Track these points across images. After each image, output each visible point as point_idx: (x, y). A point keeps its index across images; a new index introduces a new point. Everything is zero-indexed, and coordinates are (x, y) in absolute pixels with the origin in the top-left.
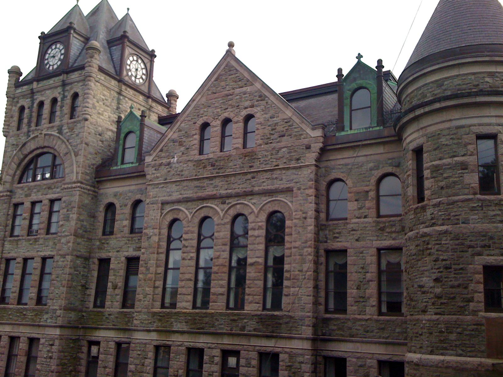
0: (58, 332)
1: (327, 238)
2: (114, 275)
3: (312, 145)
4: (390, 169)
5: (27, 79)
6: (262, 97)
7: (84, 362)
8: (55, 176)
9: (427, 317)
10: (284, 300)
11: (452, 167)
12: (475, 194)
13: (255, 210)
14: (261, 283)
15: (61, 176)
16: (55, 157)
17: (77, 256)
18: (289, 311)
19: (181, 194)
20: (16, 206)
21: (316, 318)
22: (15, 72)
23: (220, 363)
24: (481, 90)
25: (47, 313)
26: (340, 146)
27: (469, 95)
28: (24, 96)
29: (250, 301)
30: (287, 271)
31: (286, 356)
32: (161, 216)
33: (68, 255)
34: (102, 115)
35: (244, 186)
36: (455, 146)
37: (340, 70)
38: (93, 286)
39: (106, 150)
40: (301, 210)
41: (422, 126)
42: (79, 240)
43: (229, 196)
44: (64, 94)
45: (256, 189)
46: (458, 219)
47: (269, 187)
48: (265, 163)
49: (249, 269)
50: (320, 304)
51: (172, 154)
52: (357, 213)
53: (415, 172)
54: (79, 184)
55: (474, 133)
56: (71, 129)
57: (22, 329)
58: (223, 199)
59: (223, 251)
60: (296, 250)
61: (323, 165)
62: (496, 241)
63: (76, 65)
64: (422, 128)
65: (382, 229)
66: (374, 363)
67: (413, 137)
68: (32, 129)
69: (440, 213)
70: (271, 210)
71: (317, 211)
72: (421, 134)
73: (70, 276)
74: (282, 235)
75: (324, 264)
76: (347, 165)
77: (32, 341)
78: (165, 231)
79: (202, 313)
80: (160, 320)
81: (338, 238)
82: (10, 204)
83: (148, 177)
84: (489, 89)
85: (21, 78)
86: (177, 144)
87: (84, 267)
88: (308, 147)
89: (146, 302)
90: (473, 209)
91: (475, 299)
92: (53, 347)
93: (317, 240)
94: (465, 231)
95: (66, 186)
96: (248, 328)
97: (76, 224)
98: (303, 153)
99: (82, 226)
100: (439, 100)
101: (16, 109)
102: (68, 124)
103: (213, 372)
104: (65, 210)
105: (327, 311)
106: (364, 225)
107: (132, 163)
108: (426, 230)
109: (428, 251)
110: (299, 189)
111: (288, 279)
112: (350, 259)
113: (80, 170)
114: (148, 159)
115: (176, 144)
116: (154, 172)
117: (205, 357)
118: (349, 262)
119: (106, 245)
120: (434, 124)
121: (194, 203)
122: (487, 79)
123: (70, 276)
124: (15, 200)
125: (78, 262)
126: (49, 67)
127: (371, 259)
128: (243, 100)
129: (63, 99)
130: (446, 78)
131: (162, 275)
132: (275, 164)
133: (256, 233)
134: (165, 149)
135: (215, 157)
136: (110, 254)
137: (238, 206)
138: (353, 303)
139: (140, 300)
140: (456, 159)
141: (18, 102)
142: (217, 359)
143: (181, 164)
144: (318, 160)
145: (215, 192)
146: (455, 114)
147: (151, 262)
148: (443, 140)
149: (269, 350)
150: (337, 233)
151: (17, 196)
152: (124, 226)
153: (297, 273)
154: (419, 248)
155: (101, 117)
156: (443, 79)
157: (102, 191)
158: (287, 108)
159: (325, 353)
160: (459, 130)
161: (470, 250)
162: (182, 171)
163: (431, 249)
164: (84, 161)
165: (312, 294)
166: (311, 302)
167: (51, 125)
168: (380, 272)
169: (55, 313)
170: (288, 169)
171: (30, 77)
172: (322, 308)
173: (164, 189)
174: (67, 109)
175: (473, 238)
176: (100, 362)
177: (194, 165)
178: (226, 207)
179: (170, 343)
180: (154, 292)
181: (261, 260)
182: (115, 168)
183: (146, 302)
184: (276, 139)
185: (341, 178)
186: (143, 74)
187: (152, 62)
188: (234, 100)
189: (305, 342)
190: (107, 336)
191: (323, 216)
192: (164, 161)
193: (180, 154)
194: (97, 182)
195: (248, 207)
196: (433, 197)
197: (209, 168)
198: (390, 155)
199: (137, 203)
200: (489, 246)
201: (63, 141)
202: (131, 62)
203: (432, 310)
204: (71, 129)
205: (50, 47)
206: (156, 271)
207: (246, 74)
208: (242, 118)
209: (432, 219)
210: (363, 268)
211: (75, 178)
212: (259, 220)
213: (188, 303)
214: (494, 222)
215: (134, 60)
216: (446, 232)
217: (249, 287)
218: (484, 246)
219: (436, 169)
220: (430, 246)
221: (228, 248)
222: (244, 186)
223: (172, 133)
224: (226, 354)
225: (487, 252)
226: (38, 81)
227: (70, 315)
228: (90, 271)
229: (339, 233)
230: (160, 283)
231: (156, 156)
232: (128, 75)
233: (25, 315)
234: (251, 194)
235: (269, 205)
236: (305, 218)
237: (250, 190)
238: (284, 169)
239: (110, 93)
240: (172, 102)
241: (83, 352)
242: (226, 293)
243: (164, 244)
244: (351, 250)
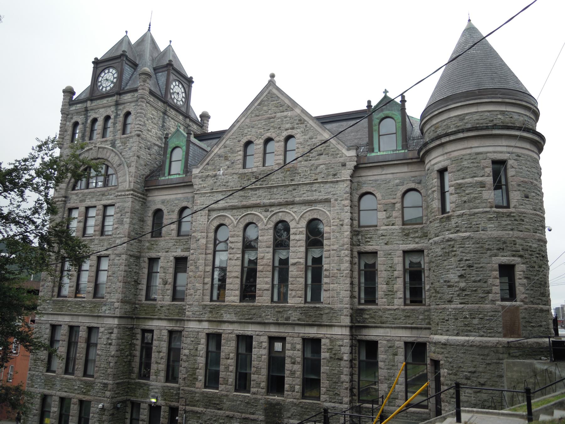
0: (116, 321)
1: (359, 242)
2: (164, 273)
3: (347, 163)
4: (413, 186)
5: (80, 98)
6: (301, 121)
7: (138, 348)
8: (107, 185)
9: (453, 306)
10: (324, 295)
11: (472, 185)
12: (491, 207)
13: (296, 217)
14: (302, 280)
15: (113, 184)
16: (107, 167)
17: (131, 256)
18: (329, 304)
19: (227, 203)
20: (70, 210)
21: (352, 309)
22: (69, 92)
23: (267, 348)
24: (495, 125)
25: (105, 305)
26: (371, 165)
27: (487, 128)
28: (78, 113)
29: (293, 295)
30: (326, 270)
31: (328, 341)
32: (208, 221)
33: (123, 254)
34: (151, 131)
35: (286, 196)
36: (474, 168)
37: (369, 102)
38: (144, 281)
39: (153, 162)
40: (338, 218)
41: (446, 151)
43: (272, 205)
44: (117, 113)
45: (297, 199)
46: (478, 227)
47: (309, 198)
48: (305, 177)
49: (291, 268)
50: (355, 297)
51: (218, 167)
52: (385, 221)
53: (439, 188)
55: (490, 158)
56: (124, 143)
57: (81, 319)
58: (266, 207)
59: (268, 253)
60: (334, 252)
61: (355, 180)
62: (509, 245)
63: (128, 87)
64: (446, 153)
65: (407, 235)
66: (402, 344)
67: (437, 160)
69: (463, 222)
70: (311, 218)
71: (352, 219)
72: (446, 158)
74: (320, 239)
75: (357, 264)
76: (376, 181)
77: (90, 330)
78: (212, 235)
79: (249, 306)
80: (211, 312)
81: (369, 242)
82: (65, 208)
83: (195, 187)
84: (501, 124)
85: (75, 97)
87: (136, 265)
88: (344, 165)
89: (197, 297)
90: (490, 219)
91: (494, 291)
92: (112, 335)
93: (352, 244)
94: (484, 237)
95: (119, 194)
96: (292, 318)
97: (130, 227)
98: (339, 170)
100: (463, 131)
101: (70, 124)
102: (121, 139)
103: (262, 355)
104: (119, 215)
105: (360, 303)
106: (392, 231)
107: (179, 174)
108: (452, 236)
109: (453, 253)
110: (336, 200)
111: (327, 277)
112: (381, 259)
113: (132, 179)
114: (195, 171)
115: (221, 158)
116: (202, 182)
117: (254, 343)
118: (379, 262)
119: (155, 246)
120: (457, 150)
121: (239, 210)
122: (499, 116)
124: (69, 205)
125: (131, 260)
126: (102, 89)
127: (398, 259)
128: (284, 122)
129: (116, 117)
130: (467, 114)
131: (210, 273)
132: (314, 178)
133: (297, 237)
134: (211, 162)
135: (259, 171)
136: (160, 254)
137: (280, 214)
138: (383, 296)
139: (191, 295)
140: (476, 179)
141: (72, 118)
142: (265, 345)
143: (226, 176)
144: (352, 176)
145: (258, 201)
146: (475, 143)
147: (199, 261)
148: (465, 163)
149: (311, 336)
150: (369, 238)
151: (72, 201)
152: (172, 230)
153: (336, 271)
154: (445, 250)
155: (150, 133)
156: (464, 114)
157: (150, 199)
158: (325, 131)
159: (359, 337)
160: (478, 156)
161: (489, 252)
162: (227, 182)
163: (456, 251)
164: (135, 172)
165: (349, 289)
166: (349, 295)
167: (104, 139)
168: (405, 270)
169: (113, 305)
170: (326, 182)
171: (83, 97)
172: (356, 300)
173: (211, 197)
174: (119, 126)
175: (491, 243)
176: (154, 348)
177: (239, 178)
178: (269, 214)
179: (221, 331)
180: (203, 287)
181: (302, 261)
182: (163, 178)
183: (197, 297)
184: (315, 157)
185: (371, 191)
186: (183, 97)
187: (190, 87)
188: (276, 123)
189: (344, 329)
190: (160, 327)
191: (356, 223)
192: (211, 173)
193: (226, 167)
194: (146, 190)
195: (290, 215)
196: (457, 209)
198: (413, 174)
199: (184, 209)
200: (503, 249)
201: (116, 154)
203: (457, 300)
204: (124, 143)
205: (103, 70)
206: (205, 269)
207: (287, 101)
208: (283, 138)
209: (457, 227)
210: (391, 267)
211: (127, 186)
212: (300, 226)
213: (236, 298)
214: (506, 230)
216: (468, 238)
217: (291, 284)
218: (499, 249)
219: (459, 187)
220: (455, 249)
221: (271, 250)
222: (286, 196)
223: (217, 149)
224: (272, 340)
225: (502, 254)
226: (92, 100)
227: (126, 307)
228: (141, 268)
229: (371, 238)
230: (208, 280)
231: (203, 169)
233: (83, 307)
234: (293, 203)
235: (309, 213)
236: (342, 225)
237: (292, 200)
238: (322, 182)
239: (157, 113)
240: (205, 121)
241: (137, 339)
242: (270, 289)
243: (211, 246)
244: (381, 252)
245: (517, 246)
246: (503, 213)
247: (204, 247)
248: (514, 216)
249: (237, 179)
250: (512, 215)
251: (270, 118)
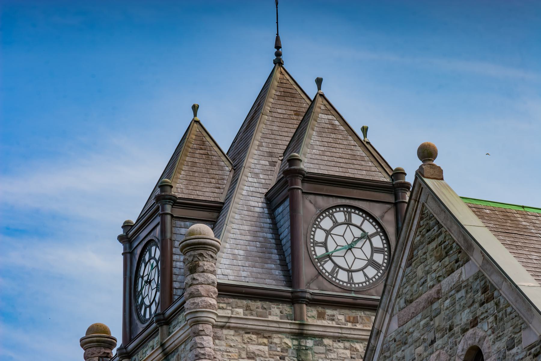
6: (488, 291)
128: (457, 307)
186: (374, 250)
202: (328, 233)
215: (336, 224)
232: (320, 273)
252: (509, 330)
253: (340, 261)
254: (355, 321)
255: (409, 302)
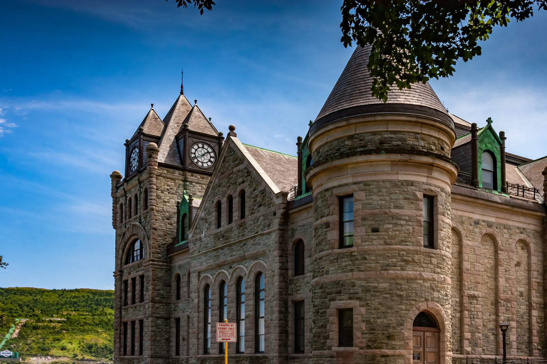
13: (247, 272)
17: (158, 318)
42: (157, 305)
54: (151, 262)
62: (346, 287)
68: (127, 221)
73: (153, 333)
78: (202, 295)
83: (191, 251)
86: (204, 221)
88: (275, 214)
90: (332, 262)
97: (153, 293)
99: (159, 294)
123: (153, 333)
132: (256, 231)
137: (238, 270)
157: (173, 265)
161: (329, 296)
170: (262, 235)
178: (232, 270)
197: (221, 239)
202: (196, 150)
208: (237, 193)
212: (249, 280)
214: (345, 272)
215: (199, 148)
232: (193, 162)
234: (243, 259)
236: (273, 276)
239: (175, 183)
243: (202, 305)
245: (356, 287)
246: (343, 254)
247: (196, 306)
248: (354, 255)
249: (213, 240)
250: (354, 254)
251: (230, 175)
252: (254, 185)
253: (199, 159)
254: (203, 178)
255: (222, 174)
